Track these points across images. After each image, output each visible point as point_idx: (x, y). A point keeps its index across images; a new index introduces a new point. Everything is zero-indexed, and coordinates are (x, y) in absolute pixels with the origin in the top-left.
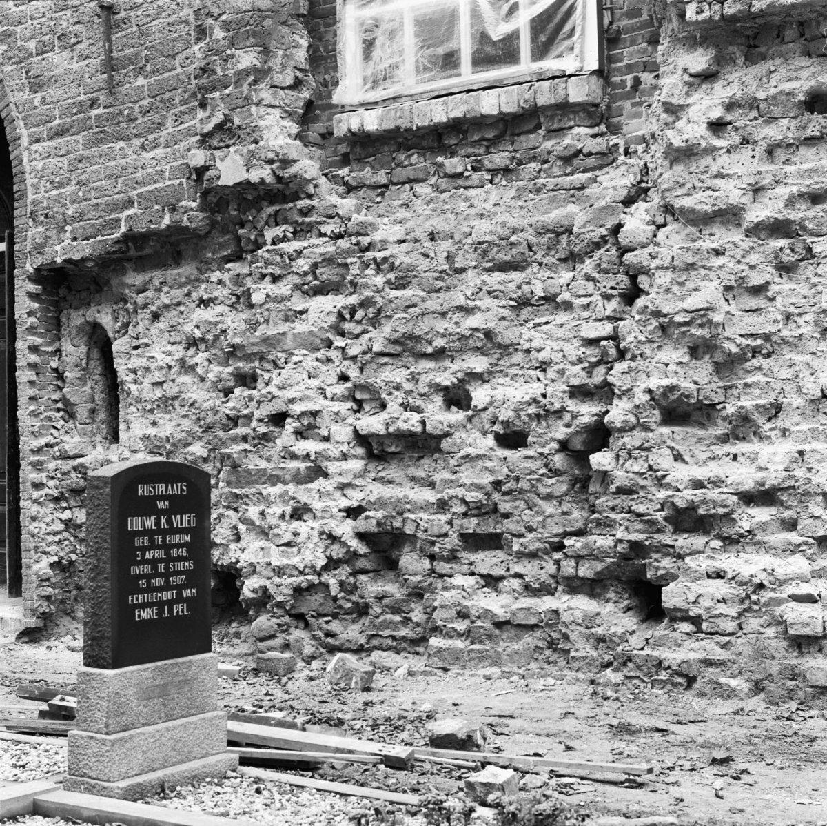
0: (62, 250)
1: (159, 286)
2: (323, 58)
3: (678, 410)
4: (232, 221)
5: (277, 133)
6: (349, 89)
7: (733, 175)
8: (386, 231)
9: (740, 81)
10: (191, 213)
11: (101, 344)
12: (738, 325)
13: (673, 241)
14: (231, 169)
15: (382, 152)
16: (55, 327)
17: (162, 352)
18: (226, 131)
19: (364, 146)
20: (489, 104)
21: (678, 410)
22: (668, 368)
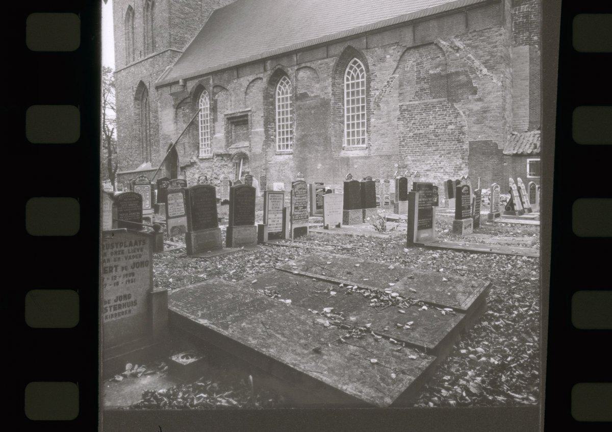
0: (182, 166)
1: (188, 169)
2: (198, 152)
3: (216, 178)
4: (192, 164)
5: (195, 158)
6: (200, 155)
7: (217, 164)
8: (201, 165)
9: (217, 158)
10: (189, 164)
11: (185, 172)
12: (218, 173)
13: (215, 168)
14: (192, 161)
15: (202, 160)
16: (182, 171)
17: (189, 173)
18: (191, 158)
19: (201, 159)
20: (207, 157)
21: (216, 178)
22: (214, 176)
